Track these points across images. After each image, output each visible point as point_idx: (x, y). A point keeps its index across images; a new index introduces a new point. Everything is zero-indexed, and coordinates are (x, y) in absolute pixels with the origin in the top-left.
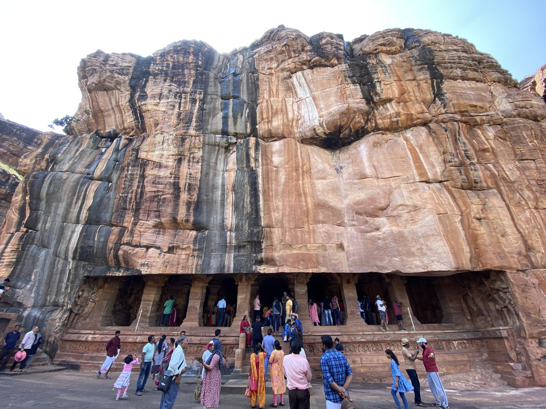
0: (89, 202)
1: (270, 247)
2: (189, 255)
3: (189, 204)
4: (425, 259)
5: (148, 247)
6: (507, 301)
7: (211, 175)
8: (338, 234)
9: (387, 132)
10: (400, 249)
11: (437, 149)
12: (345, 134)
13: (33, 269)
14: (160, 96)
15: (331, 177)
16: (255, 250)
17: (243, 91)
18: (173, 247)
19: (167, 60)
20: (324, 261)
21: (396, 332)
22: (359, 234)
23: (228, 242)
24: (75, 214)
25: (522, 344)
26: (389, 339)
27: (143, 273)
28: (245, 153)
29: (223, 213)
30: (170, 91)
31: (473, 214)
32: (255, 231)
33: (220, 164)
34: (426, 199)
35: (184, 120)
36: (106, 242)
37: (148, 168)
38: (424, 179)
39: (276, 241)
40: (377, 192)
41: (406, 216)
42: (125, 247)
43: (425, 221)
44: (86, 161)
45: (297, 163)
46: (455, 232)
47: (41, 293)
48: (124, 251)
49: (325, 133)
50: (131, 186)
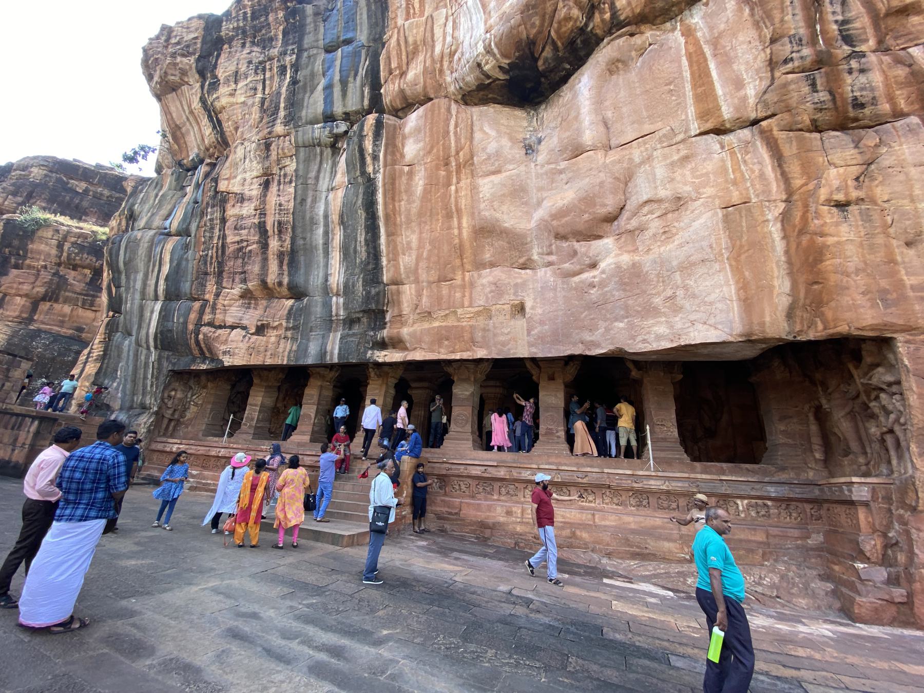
0: (166, 269)
1: (399, 318)
2: (280, 336)
3: (280, 255)
4: (677, 319)
5: (233, 327)
6: (892, 416)
7: (309, 200)
8: (516, 285)
9: (643, 28)
10: (630, 302)
11: (756, 36)
12: (546, 60)
13: (119, 362)
14: (236, 77)
15: (511, 167)
16: (375, 325)
17: (361, 23)
18: (263, 325)
19: (245, 7)
20: (483, 337)
21: (606, 471)
22: (559, 281)
23: (334, 313)
24: (153, 287)
25: (906, 524)
26: (585, 481)
27: (226, 364)
28: (357, 148)
29: (326, 265)
30: (250, 62)
31: (823, 194)
32: (373, 291)
33: (324, 178)
34: (707, 174)
35: (269, 110)
36: (185, 323)
37: (228, 206)
38: (709, 125)
39: (406, 308)
40: (598, 181)
41: (655, 226)
42: (205, 329)
43: (691, 229)
44: (164, 212)
45: (446, 148)
46: (759, 246)
47: (128, 392)
48: (205, 335)
49: (500, 67)
50: (211, 238)
